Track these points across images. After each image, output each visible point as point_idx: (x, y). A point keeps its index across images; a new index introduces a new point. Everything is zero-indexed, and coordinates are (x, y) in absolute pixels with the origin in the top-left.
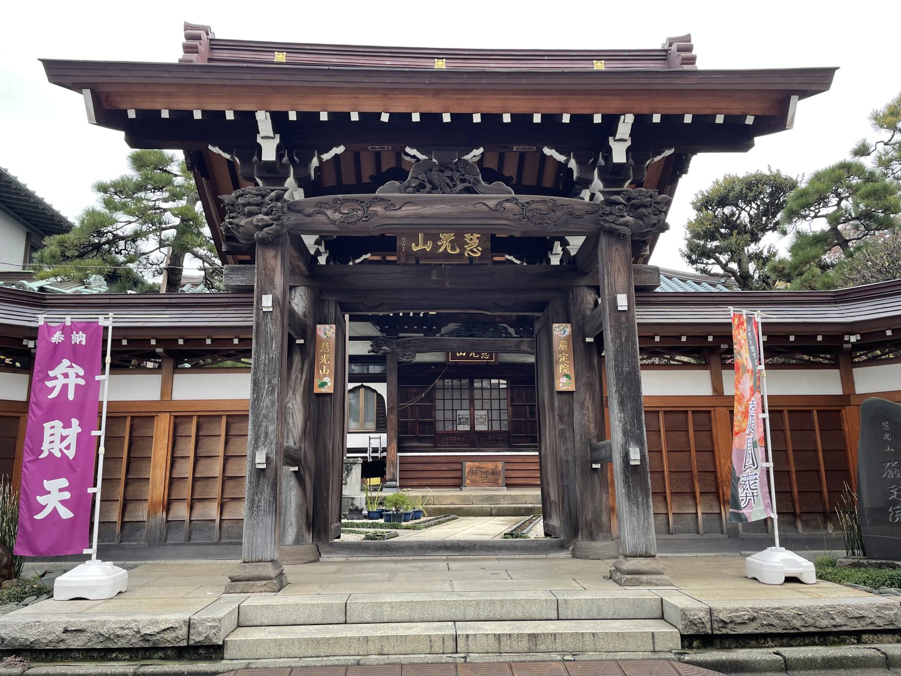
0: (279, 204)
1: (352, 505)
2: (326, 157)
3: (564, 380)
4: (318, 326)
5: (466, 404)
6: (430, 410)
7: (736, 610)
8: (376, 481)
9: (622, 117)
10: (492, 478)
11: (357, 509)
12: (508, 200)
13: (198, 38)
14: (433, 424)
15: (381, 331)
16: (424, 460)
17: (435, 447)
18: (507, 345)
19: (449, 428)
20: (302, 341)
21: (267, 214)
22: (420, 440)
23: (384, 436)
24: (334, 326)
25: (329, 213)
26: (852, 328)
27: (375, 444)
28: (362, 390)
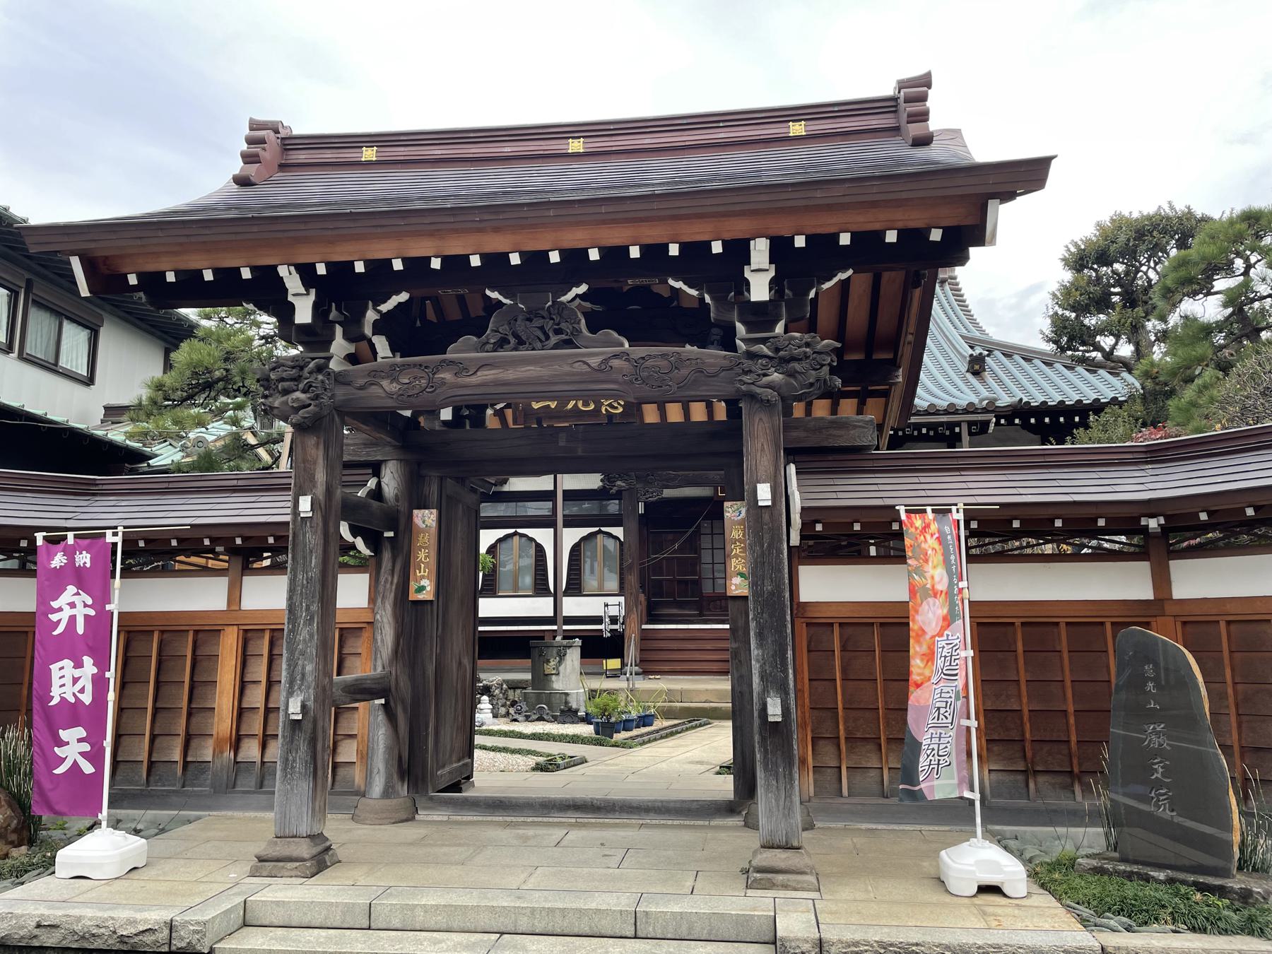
0: (320, 377)
1: (566, 703)
2: (385, 307)
3: (737, 580)
4: (415, 512)
7: (856, 944)
8: (614, 663)
9: (752, 243)
11: (570, 710)
12: (615, 356)
13: (262, 141)
14: (697, 583)
16: (681, 635)
17: (700, 615)
20: (391, 534)
21: (304, 391)
22: (680, 605)
23: (622, 599)
24: (434, 511)
25: (385, 383)
26: (1152, 508)
27: (613, 611)
28: (599, 537)
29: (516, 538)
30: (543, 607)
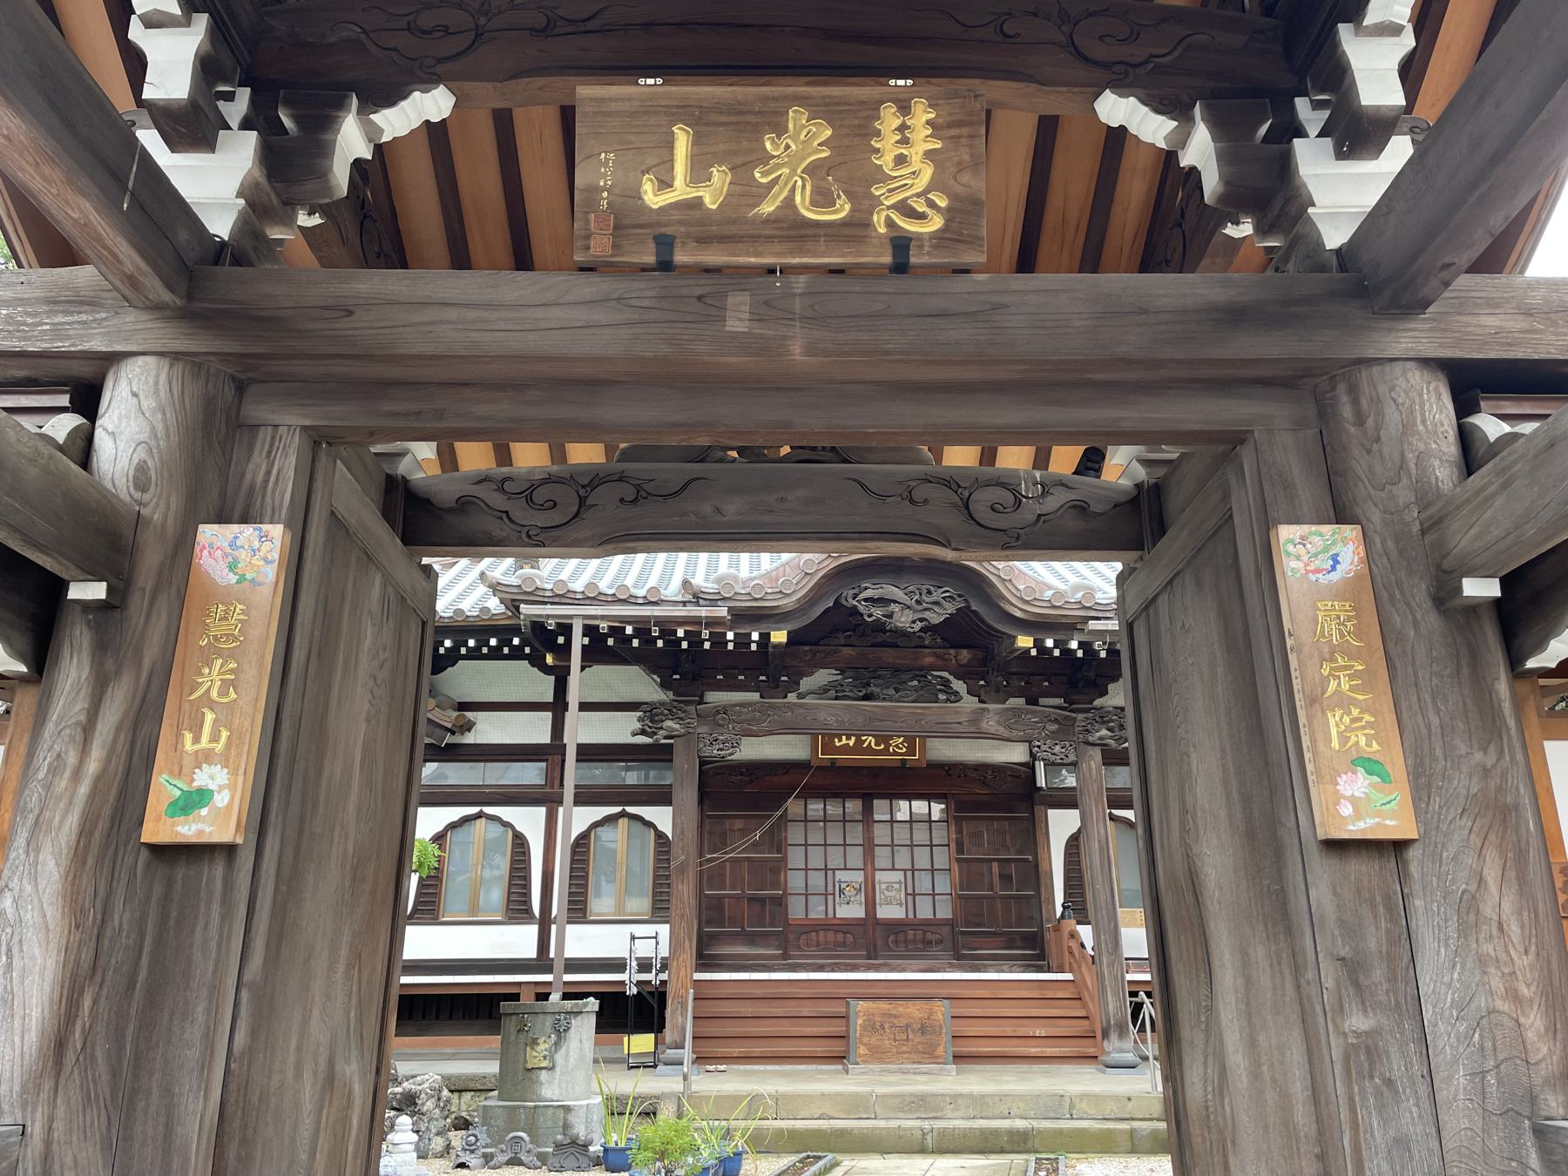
1: (566, 1126)
3: (1355, 785)
4: (208, 533)
5: (856, 856)
6: (777, 869)
8: (642, 1043)
10: (920, 1046)
11: (574, 1142)
14: (780, 902)
15: (665, 685)
16: (759, 992)
17: (785, 956)
18: (949, 719)
19: (817, 912)
20: (96, 591)
22: (751, 939)
23: (664, 930)
24: (276, 531)
27: (644, 949)
28: (623, 822)
30: (520, 941)
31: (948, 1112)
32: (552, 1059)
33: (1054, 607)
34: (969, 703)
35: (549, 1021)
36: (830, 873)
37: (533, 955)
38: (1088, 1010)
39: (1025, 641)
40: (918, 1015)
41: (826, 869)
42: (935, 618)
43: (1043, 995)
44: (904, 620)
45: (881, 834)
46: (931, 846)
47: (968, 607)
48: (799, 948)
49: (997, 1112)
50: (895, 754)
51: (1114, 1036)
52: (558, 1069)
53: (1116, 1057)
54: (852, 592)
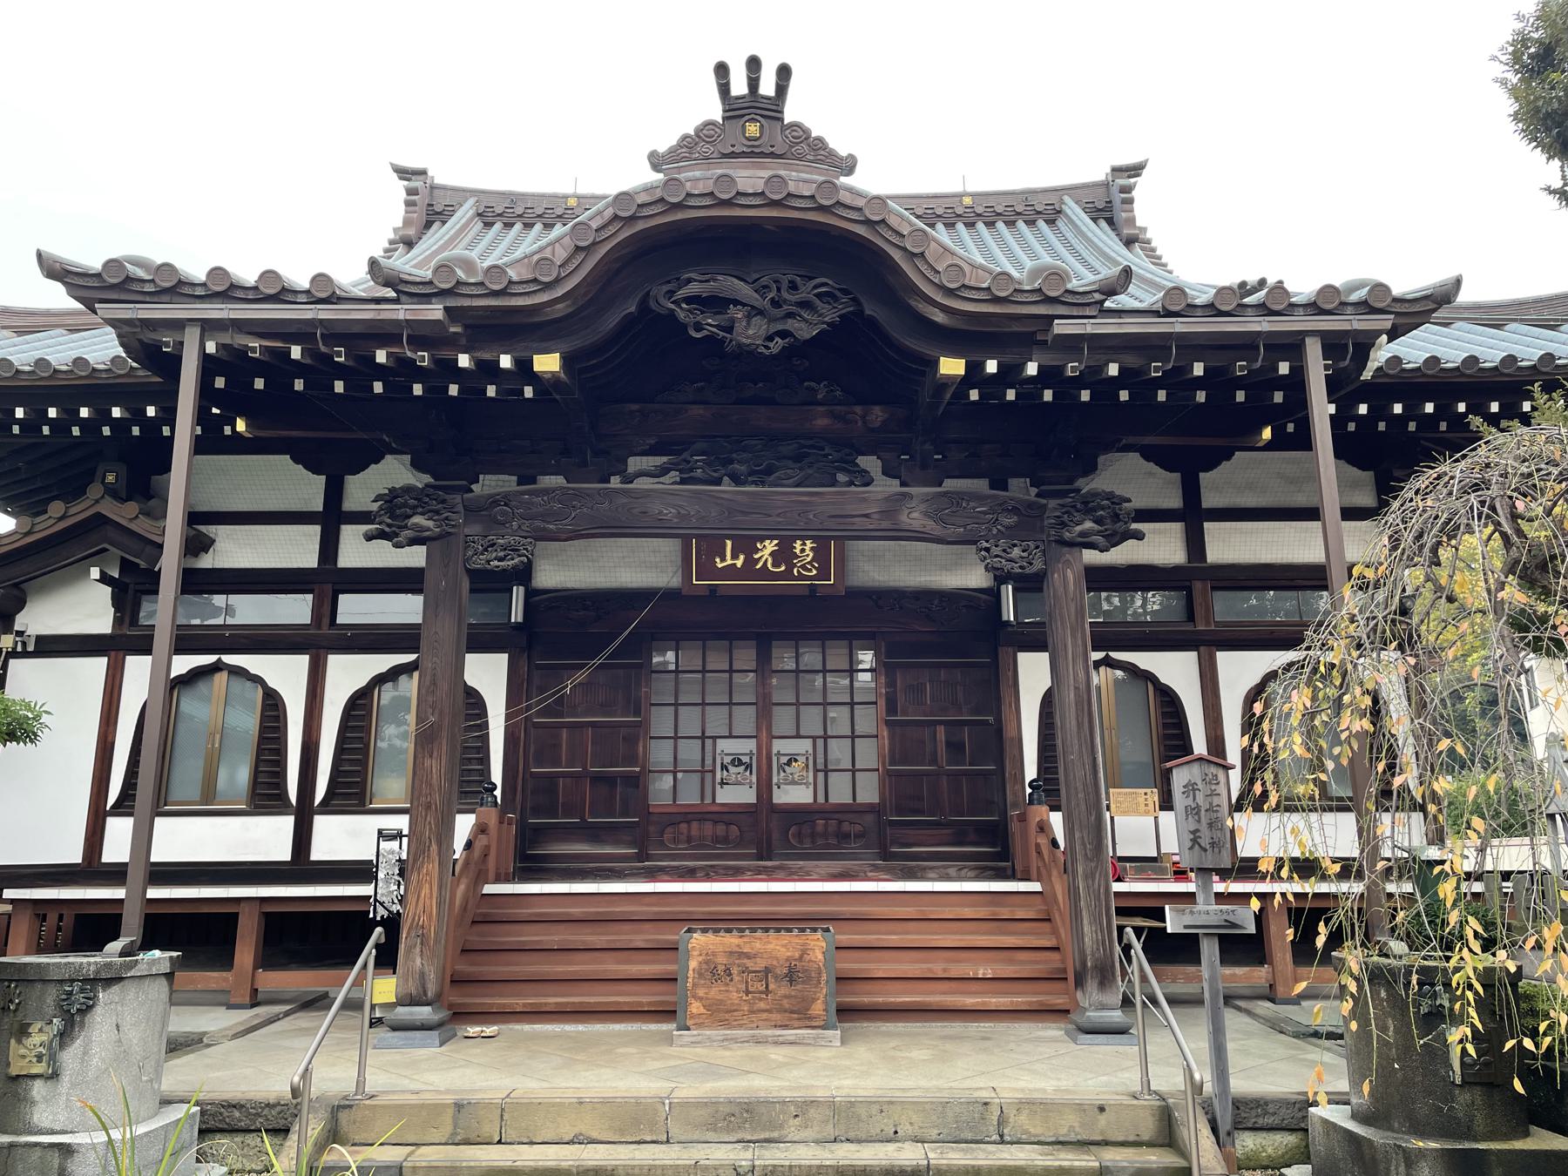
5: (745, 718)
6: (633, 738)
10: (789, 1002)
14: (636, 783)
15: (417, 465)
16: (576, 911)
17: (641, 857)
18: (851, 509)
19: (690, 797)
29: (221, 678)
30: (269, 838)
31: (792, 1129)
32: (53, 1058)
33: (997, 300)
34: (886, 486)
35: (51, 995)
36: (709, 742)
37: (285, 855)
38: (1058, 937)
39: (952, 366)
40: (784, 953)
41: (703, 737)
42: (805, 330)
43: (996, 912)
44: (751, 333)
45: (781, 690)
46: (852, 704)
47: (860, 313)
48: (662, 845)
49: (875, 1131)
50: (801, 577)
51: (1092, 985)
52: (66, 1079)
53: (1094, 1016)
54: (665, 288)
